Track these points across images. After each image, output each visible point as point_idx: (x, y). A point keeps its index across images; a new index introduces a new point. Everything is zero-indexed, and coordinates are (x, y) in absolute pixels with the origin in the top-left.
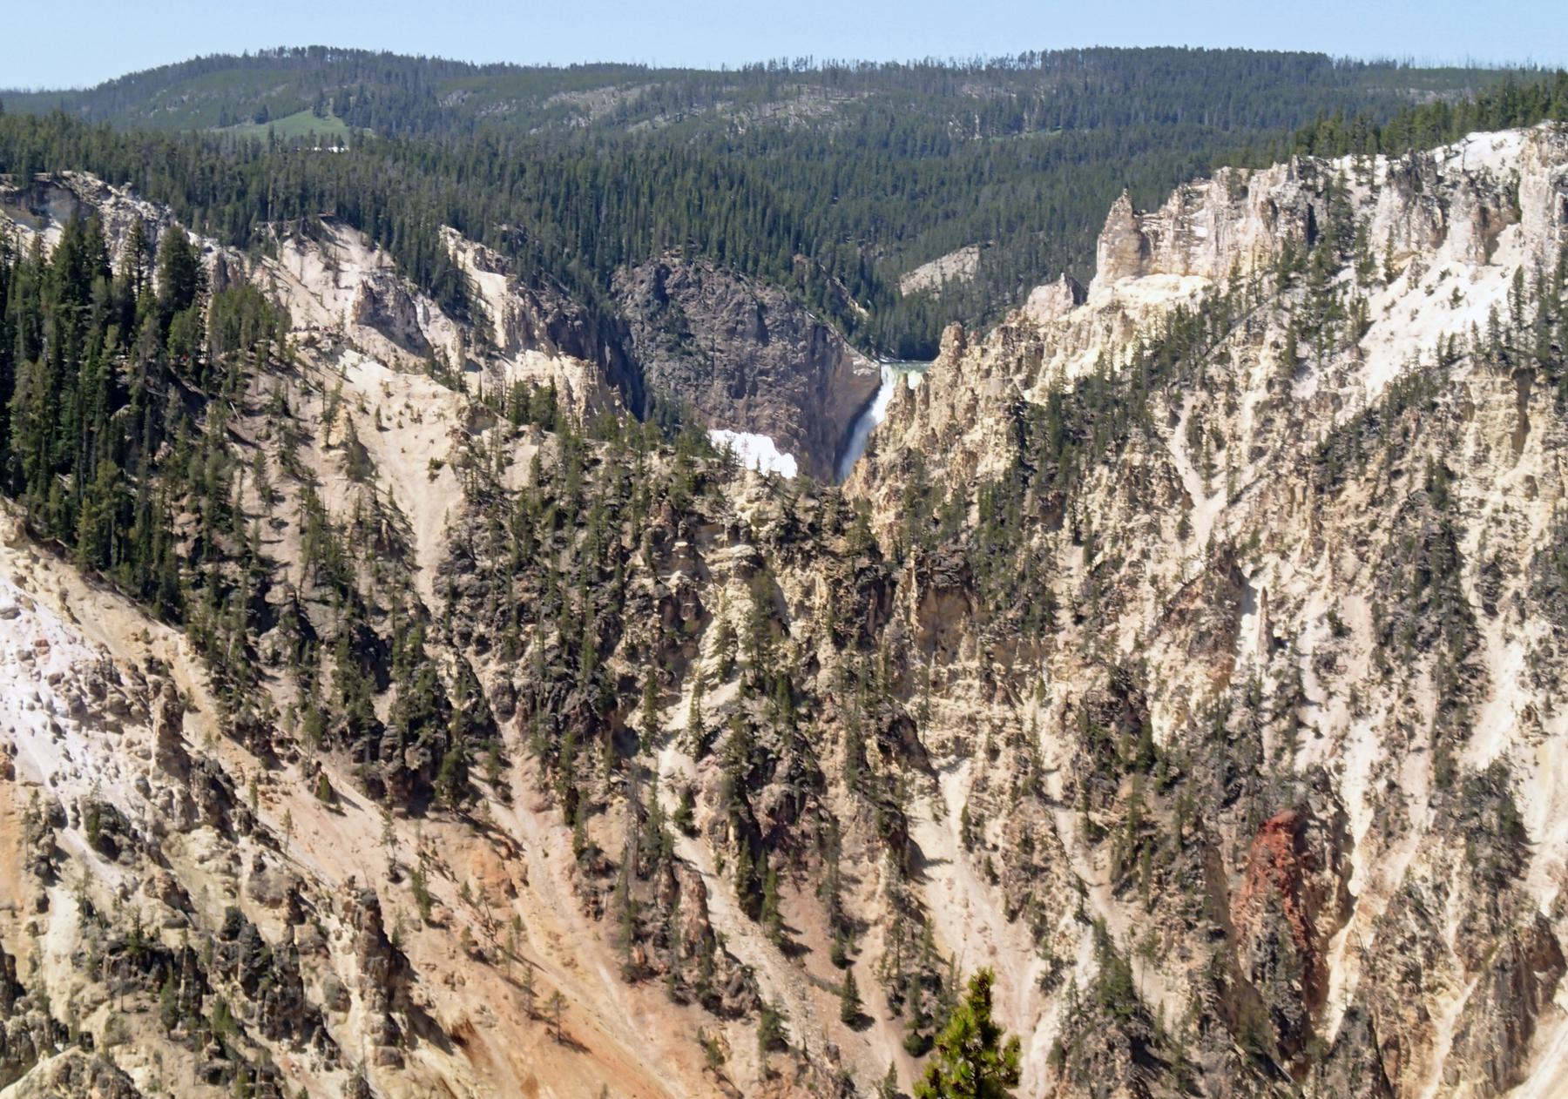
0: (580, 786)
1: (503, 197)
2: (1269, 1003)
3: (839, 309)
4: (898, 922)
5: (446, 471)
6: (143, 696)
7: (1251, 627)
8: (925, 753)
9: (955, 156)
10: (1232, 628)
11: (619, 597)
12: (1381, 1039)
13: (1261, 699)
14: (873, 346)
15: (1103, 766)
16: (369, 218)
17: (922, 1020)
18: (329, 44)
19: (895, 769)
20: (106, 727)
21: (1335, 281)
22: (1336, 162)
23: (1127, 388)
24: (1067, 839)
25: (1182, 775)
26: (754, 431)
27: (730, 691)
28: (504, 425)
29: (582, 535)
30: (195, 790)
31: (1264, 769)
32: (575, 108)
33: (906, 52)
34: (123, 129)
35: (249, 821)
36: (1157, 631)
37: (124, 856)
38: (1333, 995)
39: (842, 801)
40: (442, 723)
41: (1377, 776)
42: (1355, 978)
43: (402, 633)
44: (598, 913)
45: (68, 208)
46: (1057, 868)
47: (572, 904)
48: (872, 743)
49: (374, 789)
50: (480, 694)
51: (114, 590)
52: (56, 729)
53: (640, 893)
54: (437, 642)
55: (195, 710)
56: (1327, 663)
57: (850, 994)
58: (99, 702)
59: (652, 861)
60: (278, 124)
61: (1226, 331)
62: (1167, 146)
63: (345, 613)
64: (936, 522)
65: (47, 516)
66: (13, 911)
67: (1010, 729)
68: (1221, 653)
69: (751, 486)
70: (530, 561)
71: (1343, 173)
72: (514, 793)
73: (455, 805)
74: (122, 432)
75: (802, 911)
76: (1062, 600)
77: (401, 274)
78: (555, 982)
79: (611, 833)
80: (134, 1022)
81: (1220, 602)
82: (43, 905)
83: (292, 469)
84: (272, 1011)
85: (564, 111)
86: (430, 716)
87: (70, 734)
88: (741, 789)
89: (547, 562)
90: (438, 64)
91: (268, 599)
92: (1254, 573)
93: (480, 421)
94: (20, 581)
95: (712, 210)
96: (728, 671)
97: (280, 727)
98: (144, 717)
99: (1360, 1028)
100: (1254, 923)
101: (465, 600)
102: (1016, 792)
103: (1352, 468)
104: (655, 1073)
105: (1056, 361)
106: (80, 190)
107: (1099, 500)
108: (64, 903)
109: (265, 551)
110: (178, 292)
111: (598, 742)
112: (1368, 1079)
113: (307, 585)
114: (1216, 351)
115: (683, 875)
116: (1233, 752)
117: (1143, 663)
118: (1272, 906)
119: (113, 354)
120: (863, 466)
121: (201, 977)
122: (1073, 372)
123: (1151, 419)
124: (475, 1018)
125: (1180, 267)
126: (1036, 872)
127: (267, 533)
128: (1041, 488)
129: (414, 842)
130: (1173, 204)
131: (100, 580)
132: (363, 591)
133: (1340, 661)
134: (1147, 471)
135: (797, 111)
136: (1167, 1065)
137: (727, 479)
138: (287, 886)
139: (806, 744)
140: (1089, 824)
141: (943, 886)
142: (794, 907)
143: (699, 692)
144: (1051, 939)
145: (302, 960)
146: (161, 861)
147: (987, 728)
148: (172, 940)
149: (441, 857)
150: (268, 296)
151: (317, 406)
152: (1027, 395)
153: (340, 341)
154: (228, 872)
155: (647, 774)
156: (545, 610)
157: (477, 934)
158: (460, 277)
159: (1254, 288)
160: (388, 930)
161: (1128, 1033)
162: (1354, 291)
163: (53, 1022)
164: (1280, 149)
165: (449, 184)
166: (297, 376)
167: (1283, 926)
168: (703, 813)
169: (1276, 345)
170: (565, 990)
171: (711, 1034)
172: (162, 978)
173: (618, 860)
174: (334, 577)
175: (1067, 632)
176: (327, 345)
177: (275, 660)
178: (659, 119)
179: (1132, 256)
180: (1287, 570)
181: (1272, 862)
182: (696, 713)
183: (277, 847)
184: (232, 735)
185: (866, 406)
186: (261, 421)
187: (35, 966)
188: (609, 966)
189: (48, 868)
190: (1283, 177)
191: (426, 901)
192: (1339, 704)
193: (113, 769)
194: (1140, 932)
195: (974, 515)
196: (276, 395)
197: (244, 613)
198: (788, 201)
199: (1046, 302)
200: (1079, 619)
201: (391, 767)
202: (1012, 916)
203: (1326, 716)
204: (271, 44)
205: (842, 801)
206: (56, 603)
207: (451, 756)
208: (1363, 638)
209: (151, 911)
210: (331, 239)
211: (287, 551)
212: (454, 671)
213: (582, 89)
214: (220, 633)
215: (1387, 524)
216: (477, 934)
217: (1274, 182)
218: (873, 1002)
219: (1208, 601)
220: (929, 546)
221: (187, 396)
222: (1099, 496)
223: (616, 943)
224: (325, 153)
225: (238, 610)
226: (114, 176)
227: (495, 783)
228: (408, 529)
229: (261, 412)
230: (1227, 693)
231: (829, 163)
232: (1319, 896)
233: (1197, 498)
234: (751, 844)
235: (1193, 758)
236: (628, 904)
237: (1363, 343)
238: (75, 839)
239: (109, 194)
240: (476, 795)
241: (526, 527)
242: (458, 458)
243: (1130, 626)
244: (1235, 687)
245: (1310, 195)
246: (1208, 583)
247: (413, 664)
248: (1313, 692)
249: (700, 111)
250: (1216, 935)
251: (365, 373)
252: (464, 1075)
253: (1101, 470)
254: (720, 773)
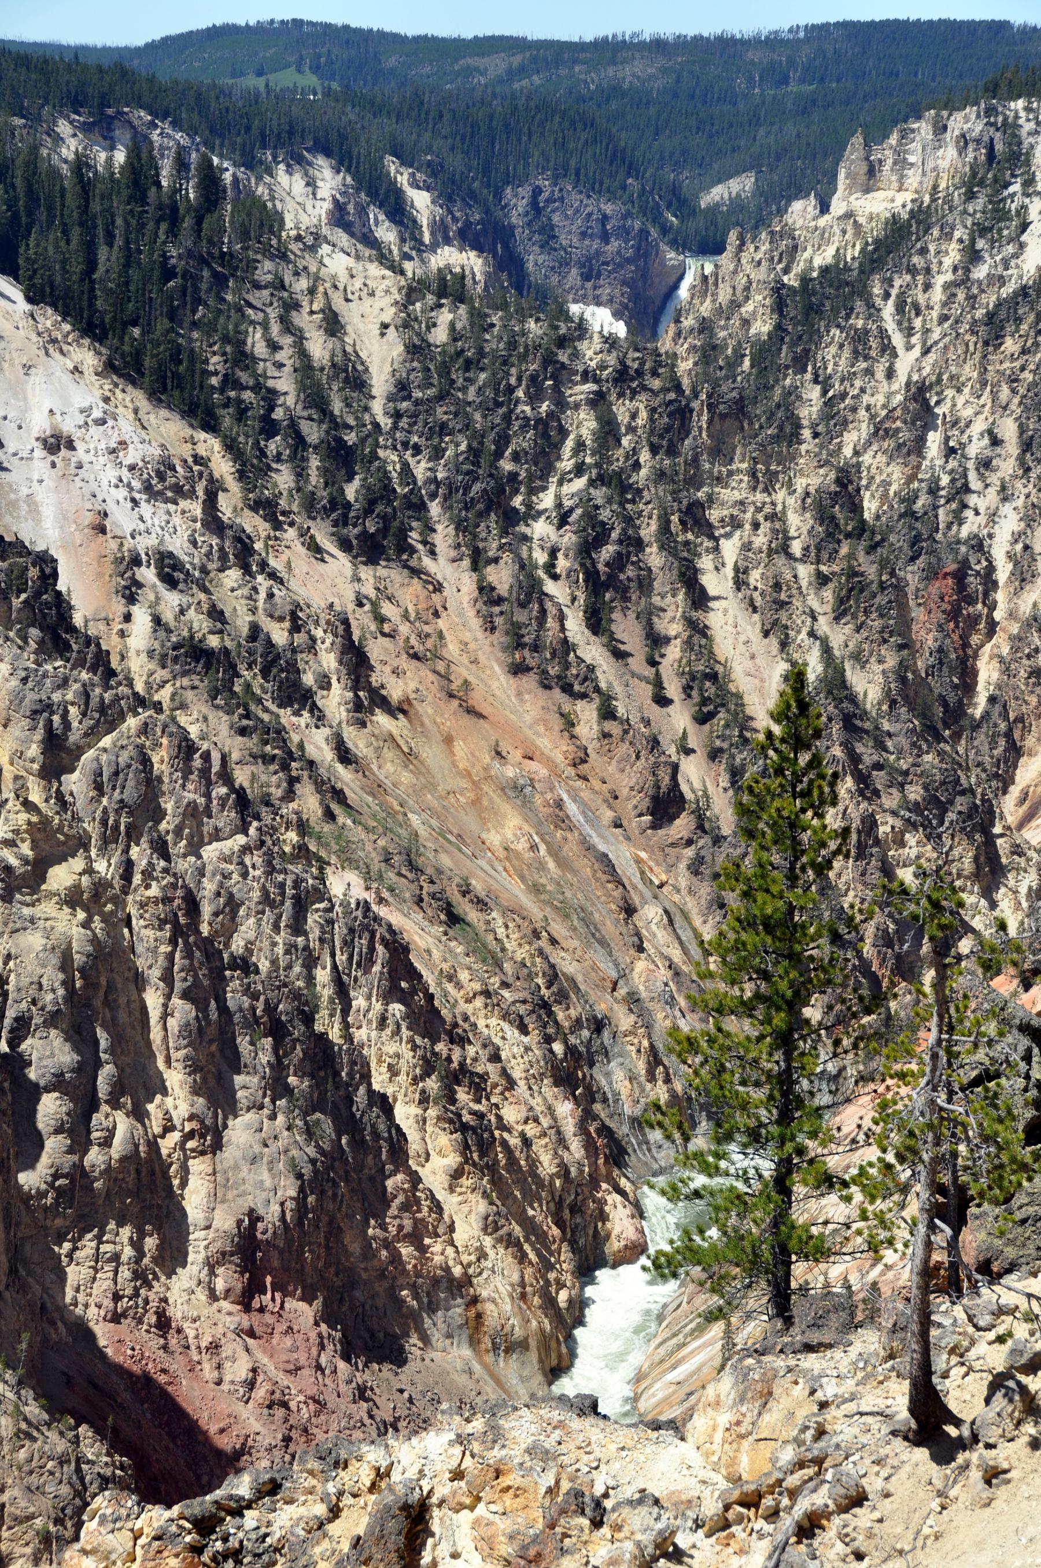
0: (481, 545)
1: (427, 136)
2: (937, 691)
3: (657, 218)
4: (690, 637)
5: (392, 329)
6: (191, 480)
7: (934, 440)
8: (710, 526)
9: (741, 106)
10: (920, 442)
11: (507, 419)
12: (1012, 716)
13: (939, 489)
14: (681, 245)
15: (830, 535)
16: (336, 149)
17: (705, 701)
18: (306, 17)
19: (690, 536)
20: (167, 501)
21: (1006, 193)
22: (1012, 104)
23: (855, 273)
24: (804, 583)
25: (883, 540)
27: (580, 483)
28: (430, 299)
29: (483, 376)
30: (227, 544)
31: (939, 536)
32: (477, 70)
33: (708, 27)
34: (164, 78)
35: (263, 565)
36: (869, 443)
37: (181, 586)
38: (980, 687)
39: (654, 557)
40: (390, 502)
41: (1016, 541)
42: (995, 676)
43: (363, 441)
44: (493, 629)
45: (128, 136)
46: (796, 603)
47: (475, 623)
48: (675, 518)
49: (345, 545)
50: (415, 483)
51: (169, 407)
52: (133, 500)
53: (521, 616)
54: (386, 447)
55: (226, 490)
56: (985, 464)
57: (658, 683)
58: (161, 483)
59: (529, 595)
60: (272, 78)
61: (926, 232)
62: (891, 95)
63: (324, 426)
64: (721, 368)
65: (123, 355)
66: (108, 622)
67: (768, 509)
68: (913, 457)
69: (597, 343)
70: (448, 393)
71: (1016, 112)
72: (438, 550)
73: (399, 556)
74: (172, 299)
75: (626, 628)
76: (805, 422)
77: (358, 190)
78: (465, 673)
79: (502, 577)
80: (189, 695)
81: (913, 423)
82: (128, 618)
83: (287, 326)
84: (280, 689)
85: (470, 72)
86: (382, 497)
87: (143, 504)
88: (587, 549)
89: (460, 395)
90: (382, 35)
91: (274, 416)
92: (938, 403)
93: (414, 296)
94: (106, 400)
95: (572, 146)
96: (579, 470)
97: (283, 502)
98: (192, 495)
99: (998, 708)
100: (927, 636)
101: (405, 420)
102: (770, 552)
103: (1010, 328)
104: (529, 733)
105: (806, 255)
106: (136, 122)
107: (833, 354)
108: (141, 617)
109: (270, 383)
110: (207, 199)
111: (493, 516)
112: (1002, 742)
113: (299, 407)
114: (918, 245)
115: (548, 605)
116: (918, 525)
117: (859, 465)
118: (940, 628)
119: (164, 243)
120: (672, 330)
121: (233, 667)
122: (818, 262)
123: (871, 295)
124: (412, 696)
125: (895, 185)
126: (782, 605)
127: (272, 371)
128: (793, 345)
129: (372, 580)
130: (893, 139)
131: (160, 401)
132: (337, 412)
133: (994, 462)
134: (866, 332)
135: (631, 73)
136: (867, 732)
137: (581, 338)
138: (288, 608)
139: (631, 519)
140: (819, 574)
141: (720, 613)
142: (622, 627)
143: (560, 483)
144: (791, 649)
145: (299, 656)
146: (206, 590)
147: (752, 509)
148: (214, 641)
149: (389, 591)
150: (269, 205)
151: (303, 284)
152: (785, 279)
153: (317, 237)
154: (250, 598)
155: (526, 538)
156: (458, 427)
157: (413, 641)
158: (398, 194)
159: (948, 200)
160: (355, 638)
161: (841, 710)
162: (1019, 200)
163: (136, 695)
164: (973, 96)
165: (390, 125)
166: (289, 262)
167: (948, 641)
168: (562, 564)
169: (961, 241)
170: (471, 679)
171: (566, 708)
172: (208, 667)
173: (506, 595)
174: (316, 400)
175: (808, 444)
176: (309, 240)
177: (278, 458)
178: (535, 78)
179: (862, 178)
180: (960, 400)
181: (942, 598)
182: (558, 497)
183: (282, 583)
184: (250, 508)
185: (676, 286)
186: (266, 293)
187: (123, 658)
188: (500, 665)
189: (131, 593)
190: (973, 116)
191: (380, 619)
192: (992, 493)
193: (174, 528)
194: (851, 645)
195: (747, 363)
196: (276, 275)
197: (257, 425)
198: (624, 139)
199: (801, 212)
200: (816, 435)
201: (356, 531)
202: (766, 634)
203: (982, 500)
204: (265, 17)
205: (654, 557)
206: (131, 416)
207: (396, 524)
208: (1012, 447)
209: (199, 622)
210: (310, 164)
211: (285, 384)
212: (398, 467)
213: (483, 55)
214: (241, 439)
215: (1032, 367)
216: (413, 641)
217: (966, 121)
218: (673, 689)
219: (905, 422)
220: (716, 385)
221: (215, 275)
222: (833, 350)
223: (505, 649)
224: (305, 103)
225: (254, 424)
226: (160, 113)
227: (425, 543)
228: (367, 369)
229: (266, 287)
230: (916, 485)
231: (652, 111)
232: (973, 621)
233: (901, 351)
234: (594, 585)
235: (890, 529)
236: (513, 624)
237: (1023, 238)
238: (148, 574)
239: (156, 126)
240: (413, 551)
241: (445, 370)
242: (399, 322)
243: (850, 440)
244: (921, 481)
245: (992, 130)
246: (905, 409)
247: (370, 462)
248: (975, 484)
249: (563, 72)
250: (901, 647)
251: (337, 262)
252: (405, 732)
253: (835, 332)
254: (574, 538)
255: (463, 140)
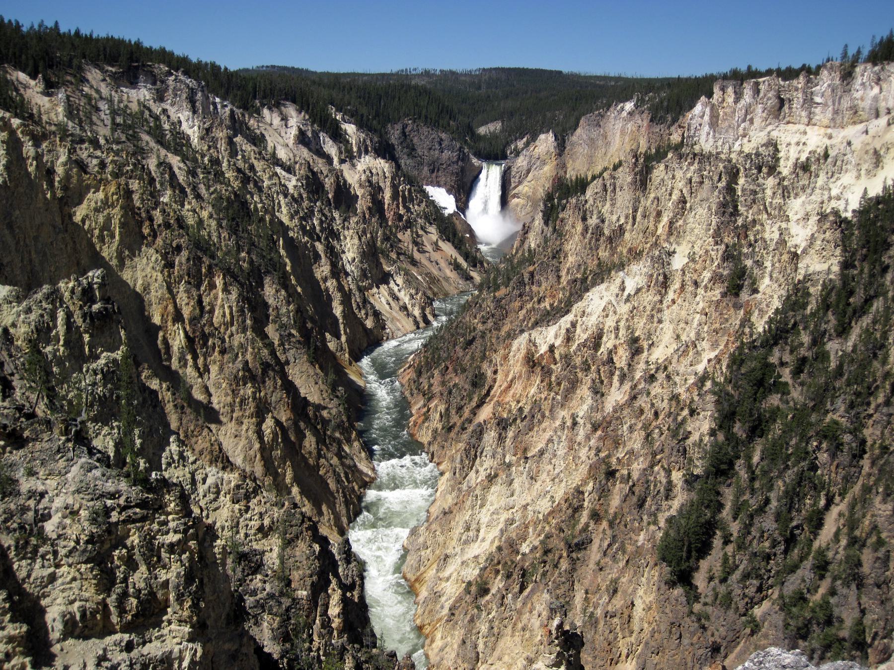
26: (439, 186)
255: (364, 98)
